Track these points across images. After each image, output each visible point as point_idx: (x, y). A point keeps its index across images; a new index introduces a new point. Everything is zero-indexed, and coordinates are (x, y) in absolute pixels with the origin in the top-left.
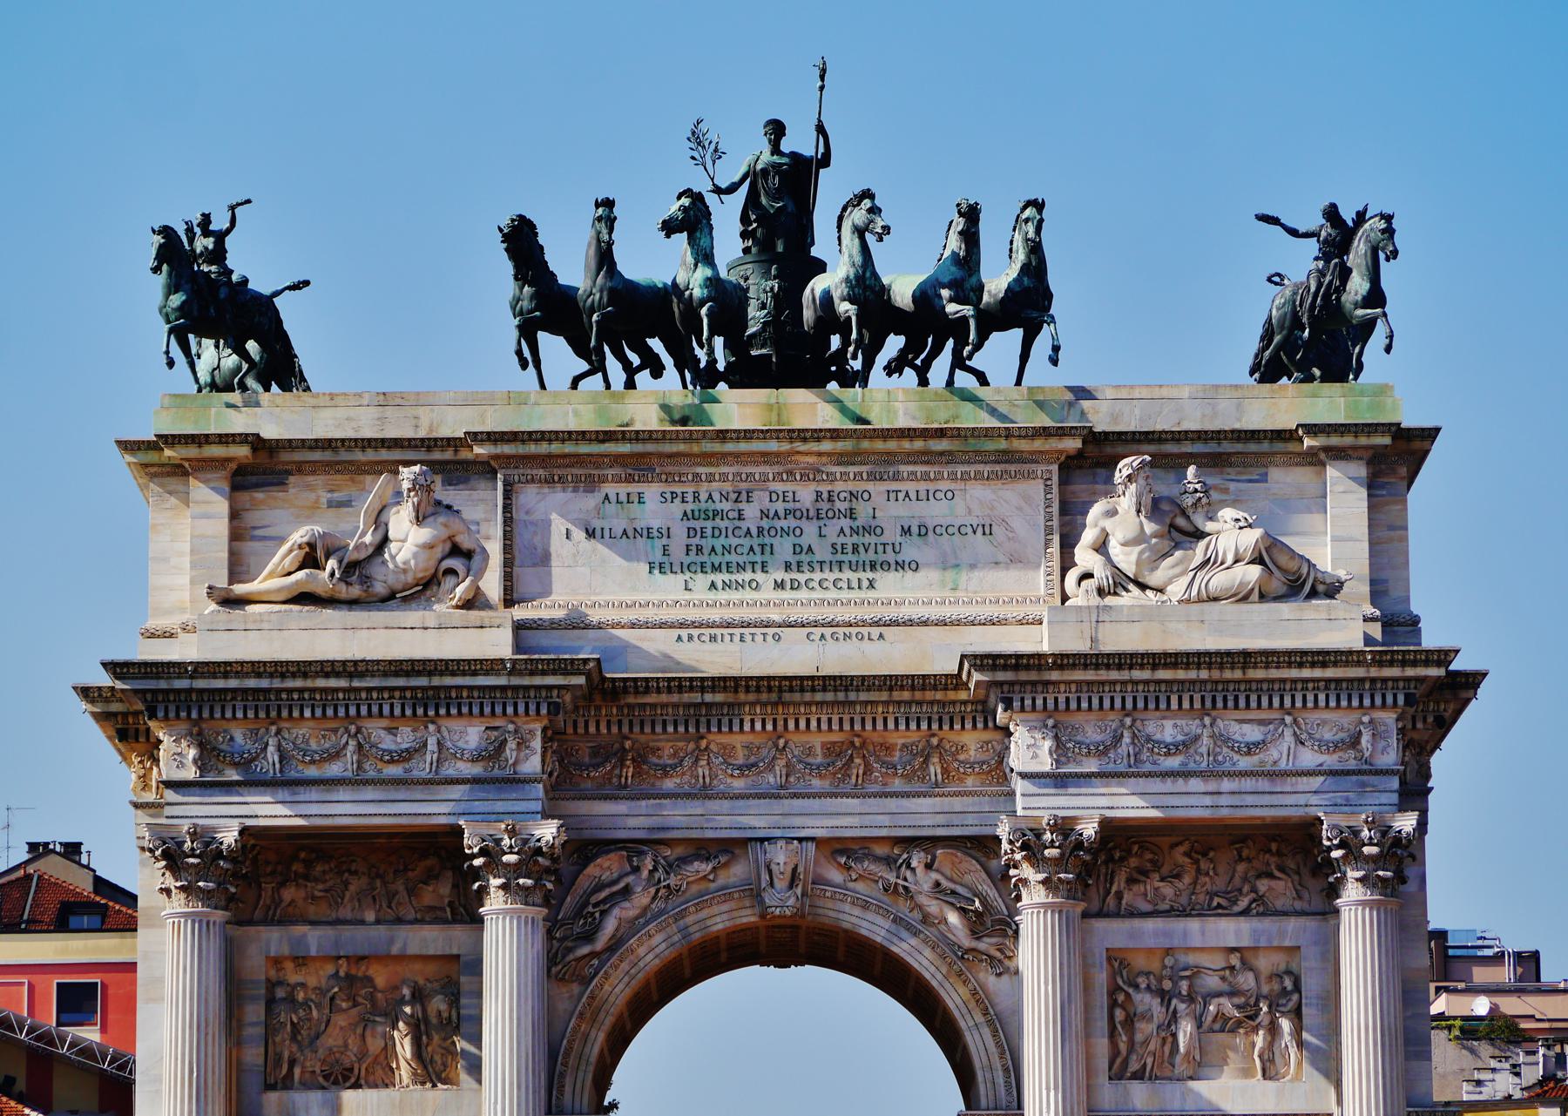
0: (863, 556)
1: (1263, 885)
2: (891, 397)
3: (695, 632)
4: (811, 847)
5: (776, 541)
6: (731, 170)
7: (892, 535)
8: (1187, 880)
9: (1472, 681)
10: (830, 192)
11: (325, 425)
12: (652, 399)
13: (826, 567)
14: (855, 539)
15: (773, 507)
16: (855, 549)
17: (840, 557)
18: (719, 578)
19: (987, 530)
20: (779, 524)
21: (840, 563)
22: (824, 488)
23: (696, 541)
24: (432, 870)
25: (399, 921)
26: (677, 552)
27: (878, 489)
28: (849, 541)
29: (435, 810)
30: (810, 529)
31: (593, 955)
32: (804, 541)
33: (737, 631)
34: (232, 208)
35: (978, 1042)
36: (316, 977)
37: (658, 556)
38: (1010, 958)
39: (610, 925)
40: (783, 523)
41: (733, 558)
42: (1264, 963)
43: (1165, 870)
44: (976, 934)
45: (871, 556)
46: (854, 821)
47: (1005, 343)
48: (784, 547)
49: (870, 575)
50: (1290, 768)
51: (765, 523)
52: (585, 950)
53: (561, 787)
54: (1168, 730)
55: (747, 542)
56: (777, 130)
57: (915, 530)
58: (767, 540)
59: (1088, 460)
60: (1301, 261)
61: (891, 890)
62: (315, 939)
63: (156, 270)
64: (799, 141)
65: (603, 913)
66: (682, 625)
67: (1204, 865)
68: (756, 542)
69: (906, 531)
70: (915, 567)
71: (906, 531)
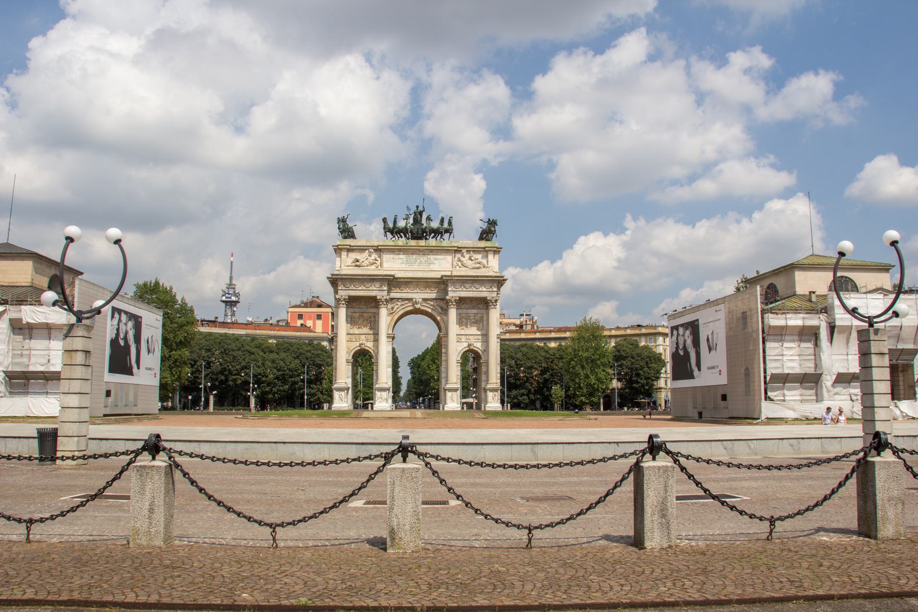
2: (432, 242)
6: (412, 212)
9: (506, 280)
10: (424, 216)
11: (359, 244)
12: (402, 241)
24: (374, 302)
29: (373, 294)
35: (442, 325)
36: (357, 315)
47: (447, 235)
50: (483, 292)
53: (389, 291)
54: (467, 286)
56: (417, 207)
59: (458, 250)
60: (485, 226)
62: (357, 310)
64: (421, 209)
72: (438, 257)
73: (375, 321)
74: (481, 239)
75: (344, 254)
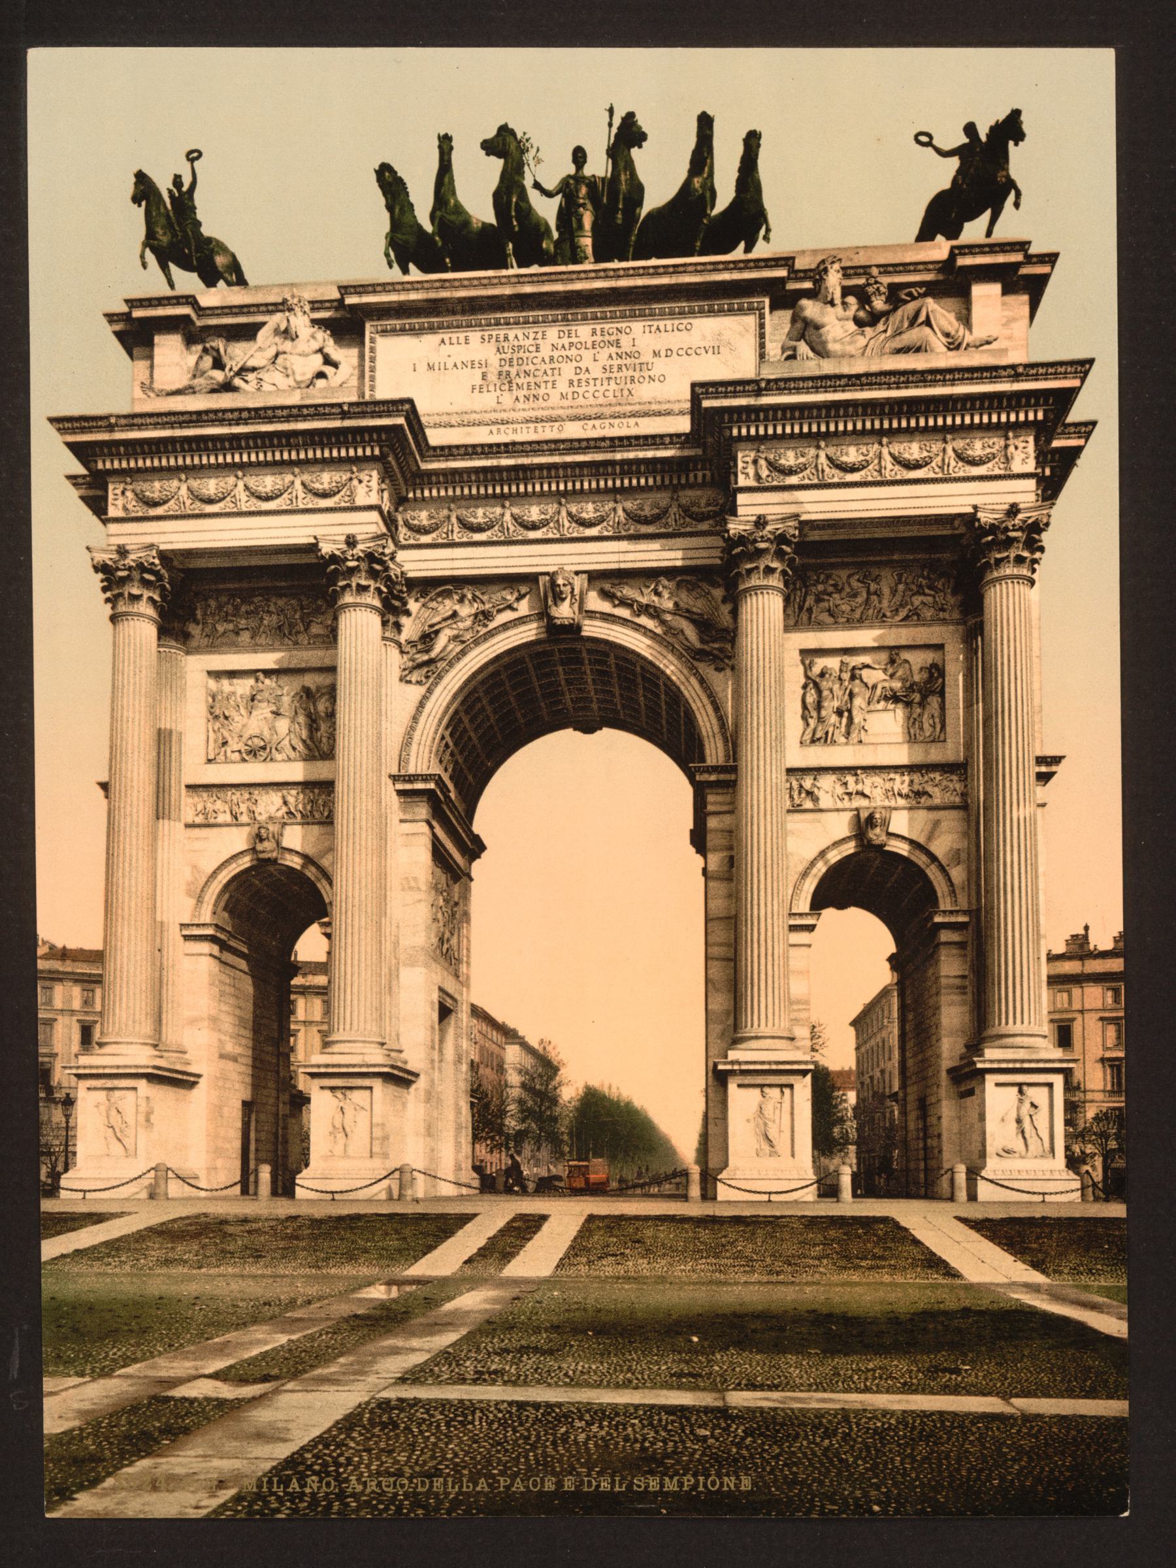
0: (625, 373)
1: (917, 600)
3: (503, 427)
4: (585, 576)
5: (563, 365)
7: (647, 357)
8: (860, 600)
13: (598, 382)
14: (619, 361)
15: (560, 342)
16: (620, 368)
17: (607, 375)
18: (521, 394)
19: (716, 350)
20: (564, 353)
21: (609, 379)
22: (598, 327)
23: (507, 368)
25: (296, 643)
26: (492, 377)
27: (637, 326)
28: (616, 362)
30: (587, 355)
31: (431, 662)
32: (583, 365)
33: (532, 425)
34: (193, 156)
37: (478, 381)
38: (729, 658)
39: (441, 641)
40: (569, 353)
41: (531, 379)
42: (918, 660)
43: (844, 594)
44: (702, 641)
45: (631, 373)
46: (615, 557)
48: (568, 370)
49: (629, 386)
51: (556, 354)
52: (426, 657)
55: (543, 367)
57: (663, 353)
58: (556, 365)
61: (645, 610)
63: (136, 199)
65: (437, 632)
66: (493, 423)
67: (873, 587)
68: (548, 367)
69: (656, 354)
70: (663, 378)
71: (656, 354)
72: (675, 340)
73: (331, 715)
74: (926, 234)
75: (168, 347)
